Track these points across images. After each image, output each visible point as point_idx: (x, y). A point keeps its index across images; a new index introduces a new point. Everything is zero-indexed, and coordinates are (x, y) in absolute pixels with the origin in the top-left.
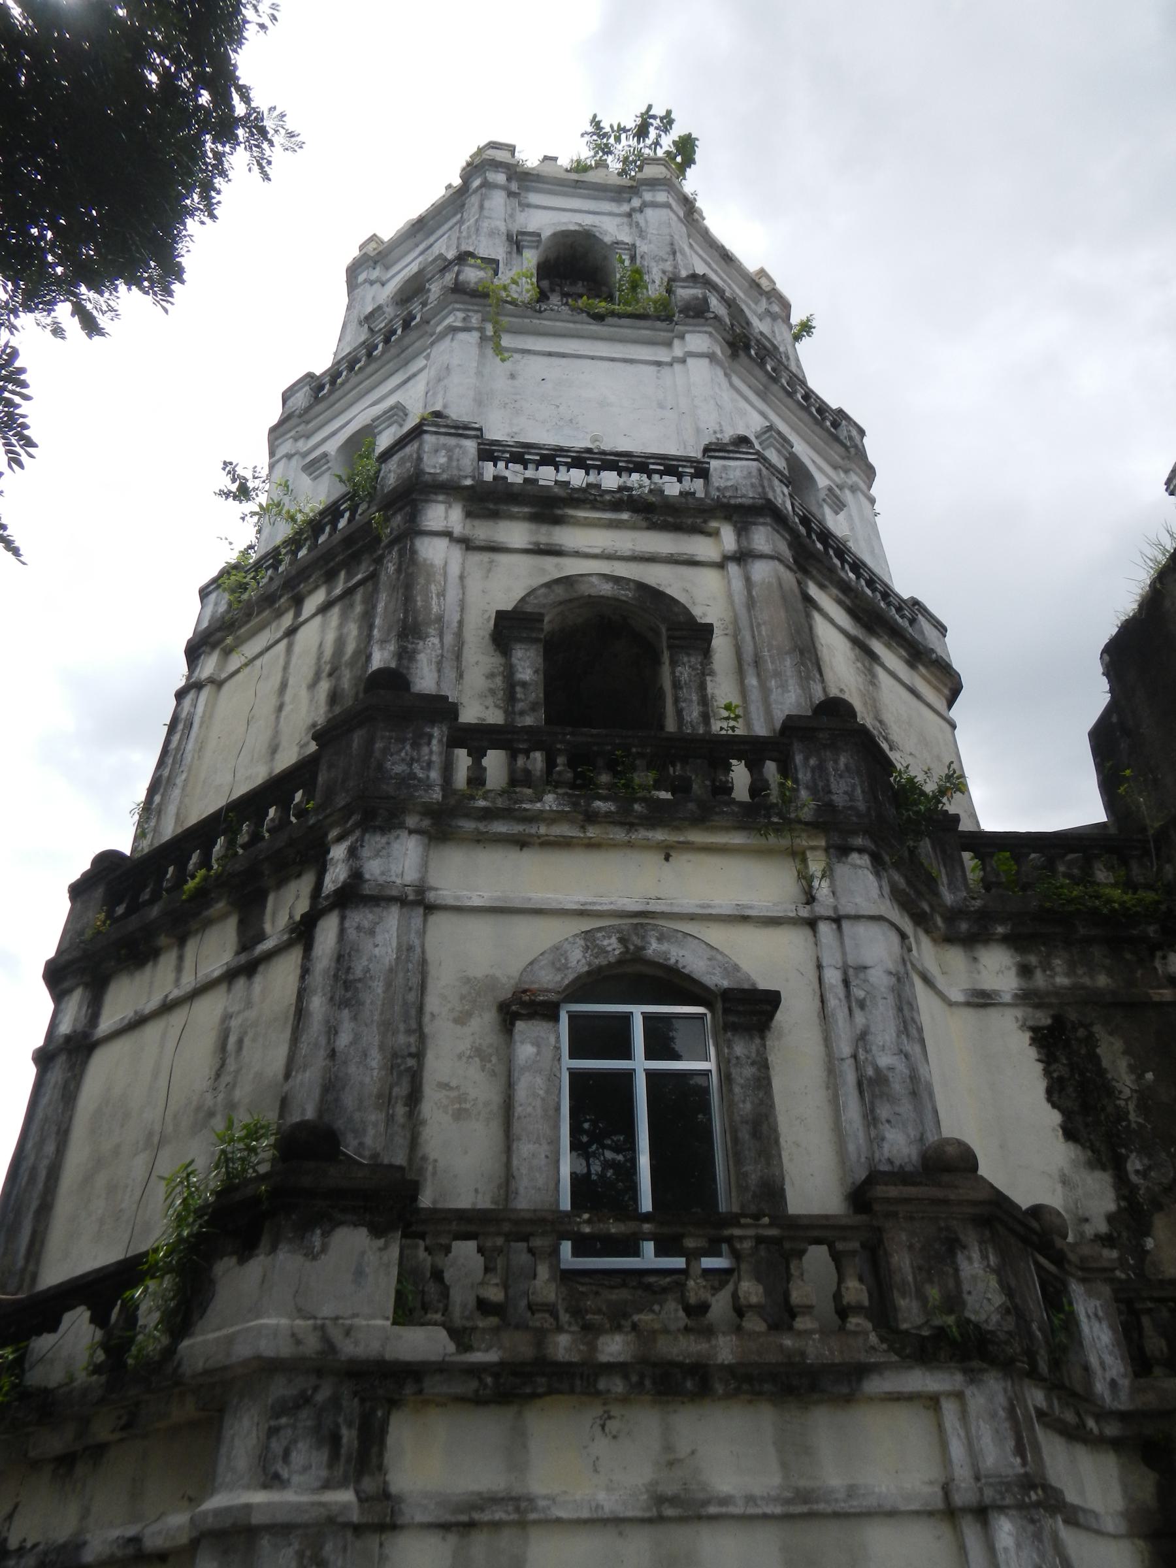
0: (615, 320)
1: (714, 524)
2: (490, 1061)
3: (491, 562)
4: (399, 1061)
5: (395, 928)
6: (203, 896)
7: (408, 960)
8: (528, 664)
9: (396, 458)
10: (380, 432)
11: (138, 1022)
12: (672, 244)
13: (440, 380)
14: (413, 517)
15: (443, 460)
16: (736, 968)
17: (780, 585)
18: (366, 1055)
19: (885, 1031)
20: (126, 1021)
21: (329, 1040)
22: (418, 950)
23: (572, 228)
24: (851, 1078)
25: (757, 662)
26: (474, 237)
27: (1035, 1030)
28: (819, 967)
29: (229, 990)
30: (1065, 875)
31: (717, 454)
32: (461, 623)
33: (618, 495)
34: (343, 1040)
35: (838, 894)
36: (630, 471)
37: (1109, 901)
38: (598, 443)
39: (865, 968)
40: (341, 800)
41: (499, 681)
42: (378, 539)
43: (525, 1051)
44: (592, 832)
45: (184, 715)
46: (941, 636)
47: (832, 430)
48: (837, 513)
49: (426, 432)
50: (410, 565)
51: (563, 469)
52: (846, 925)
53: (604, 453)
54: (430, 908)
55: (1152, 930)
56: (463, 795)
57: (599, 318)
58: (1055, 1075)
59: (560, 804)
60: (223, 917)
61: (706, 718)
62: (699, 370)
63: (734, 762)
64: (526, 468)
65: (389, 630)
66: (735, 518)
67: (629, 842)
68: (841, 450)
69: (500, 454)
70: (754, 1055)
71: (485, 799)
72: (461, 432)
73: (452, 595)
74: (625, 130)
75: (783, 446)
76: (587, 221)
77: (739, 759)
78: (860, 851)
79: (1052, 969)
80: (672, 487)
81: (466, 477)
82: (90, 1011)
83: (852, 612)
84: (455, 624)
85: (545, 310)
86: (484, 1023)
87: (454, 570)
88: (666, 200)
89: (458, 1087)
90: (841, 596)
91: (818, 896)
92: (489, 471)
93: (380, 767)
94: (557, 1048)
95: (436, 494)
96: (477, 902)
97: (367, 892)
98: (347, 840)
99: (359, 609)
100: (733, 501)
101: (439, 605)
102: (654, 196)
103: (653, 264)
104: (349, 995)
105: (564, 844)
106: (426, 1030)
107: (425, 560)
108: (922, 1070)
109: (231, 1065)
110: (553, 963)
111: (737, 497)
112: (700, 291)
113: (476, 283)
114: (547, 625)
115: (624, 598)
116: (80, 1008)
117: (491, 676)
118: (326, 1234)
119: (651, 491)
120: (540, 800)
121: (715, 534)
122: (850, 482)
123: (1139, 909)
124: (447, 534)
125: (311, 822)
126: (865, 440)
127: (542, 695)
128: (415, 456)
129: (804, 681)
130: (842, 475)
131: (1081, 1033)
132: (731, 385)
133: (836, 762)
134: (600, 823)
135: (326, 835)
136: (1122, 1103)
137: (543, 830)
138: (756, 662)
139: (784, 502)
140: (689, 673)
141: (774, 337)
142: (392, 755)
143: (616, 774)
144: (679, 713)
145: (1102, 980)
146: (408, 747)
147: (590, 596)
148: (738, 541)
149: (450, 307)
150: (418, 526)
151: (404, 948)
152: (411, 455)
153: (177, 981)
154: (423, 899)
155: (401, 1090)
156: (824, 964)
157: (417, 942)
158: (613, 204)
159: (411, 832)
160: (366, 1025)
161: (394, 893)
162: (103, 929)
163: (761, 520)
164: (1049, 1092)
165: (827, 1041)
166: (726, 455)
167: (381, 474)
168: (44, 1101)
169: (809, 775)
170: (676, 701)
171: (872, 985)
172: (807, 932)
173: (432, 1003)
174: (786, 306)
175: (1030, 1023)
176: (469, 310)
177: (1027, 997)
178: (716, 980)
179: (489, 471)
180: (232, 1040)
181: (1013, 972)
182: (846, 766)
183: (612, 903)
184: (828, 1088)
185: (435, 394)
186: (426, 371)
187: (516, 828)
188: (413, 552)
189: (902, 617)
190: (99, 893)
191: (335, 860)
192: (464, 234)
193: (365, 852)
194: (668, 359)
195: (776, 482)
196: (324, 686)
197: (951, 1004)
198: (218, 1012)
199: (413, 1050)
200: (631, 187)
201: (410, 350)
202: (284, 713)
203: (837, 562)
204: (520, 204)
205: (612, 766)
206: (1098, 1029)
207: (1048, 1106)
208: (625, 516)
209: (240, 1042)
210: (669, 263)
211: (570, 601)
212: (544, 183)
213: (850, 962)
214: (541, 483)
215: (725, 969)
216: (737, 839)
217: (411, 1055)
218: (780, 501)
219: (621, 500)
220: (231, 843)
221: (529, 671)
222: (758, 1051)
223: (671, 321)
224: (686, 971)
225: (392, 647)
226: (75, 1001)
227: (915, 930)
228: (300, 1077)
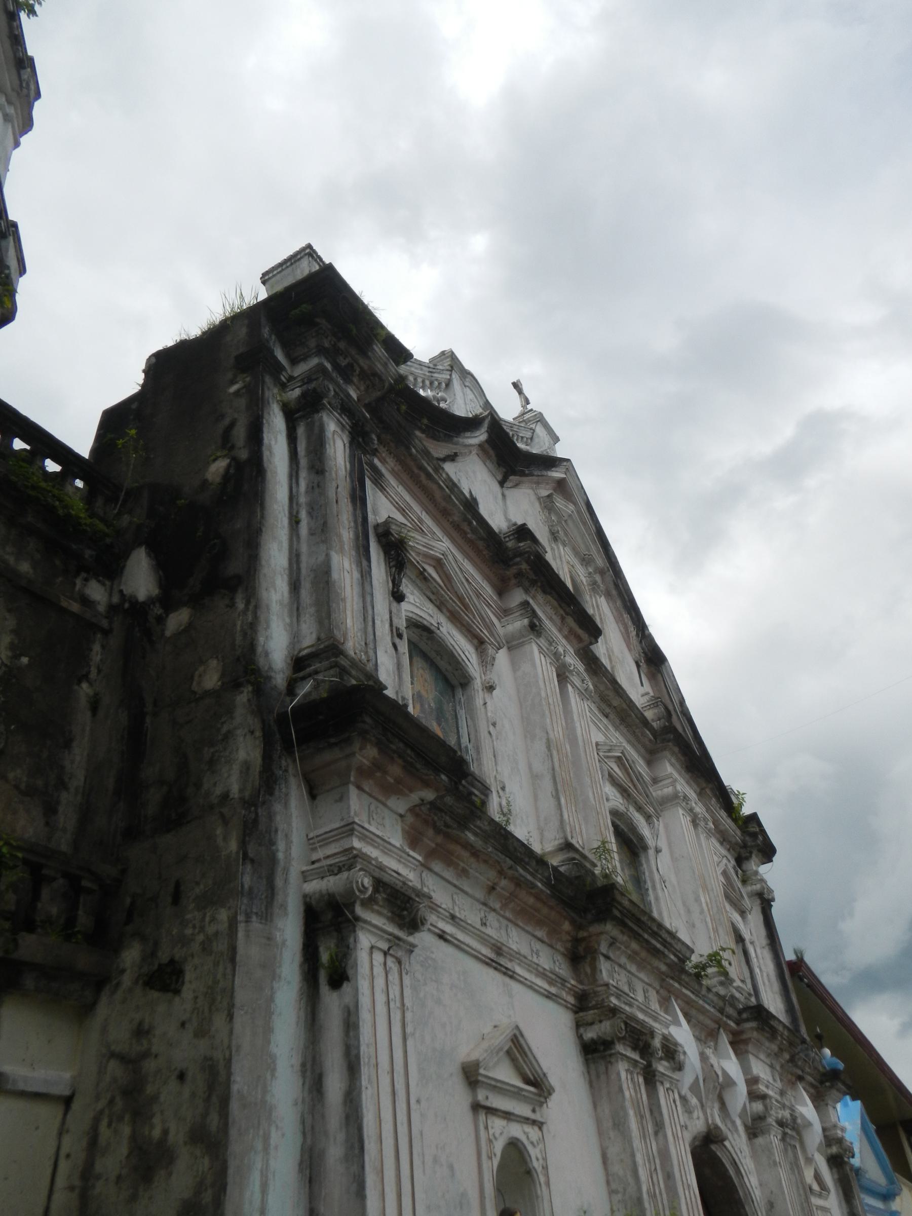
55: (88, 553)
68: (17, 82)
123: (88, 529)
145: (25, 567)
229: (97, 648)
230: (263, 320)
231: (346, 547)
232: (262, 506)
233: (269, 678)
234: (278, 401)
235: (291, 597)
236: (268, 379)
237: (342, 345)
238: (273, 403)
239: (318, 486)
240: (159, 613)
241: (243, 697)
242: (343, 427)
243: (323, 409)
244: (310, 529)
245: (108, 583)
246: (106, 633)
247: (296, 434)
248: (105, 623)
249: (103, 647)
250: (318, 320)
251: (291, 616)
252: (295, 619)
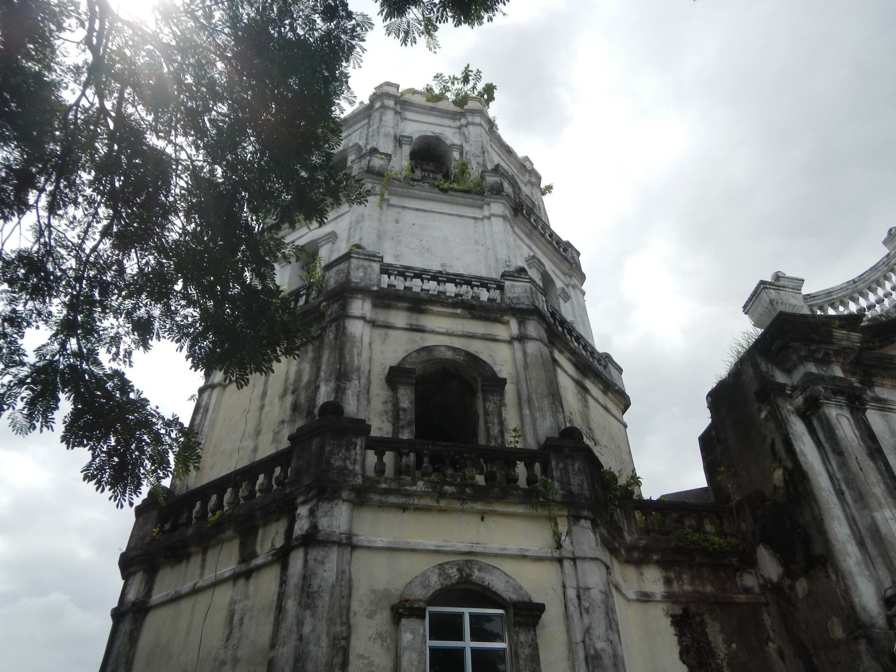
0: (454, 193)
1: (506, 318)
2: (386, 641)
3: (386, 334)
4: (337, 642)
5: (335, 560)
6: (219, 526)
7: (342, 580)
8: (406, 397)
9: (334, 270)
10: (321, 246)
11: (177, 598)
12: (483, 147)
13: (358, 222)
14: (344, 307)
15: (361, 274)
16: (521, 588)
17: (542, 356)
18: (319, 639)
19: (599, 628)
20: (169, 597)
21: (299, 628)
22: (347, 573)
23: (429, 134)
24: (581, 655)
25: (529, 401)
26: (376, 137)
27: (673, 616)
28: (564, 587)
29: (234, 585)
30: (689, 527)
31: (509, 278)
32: (369, 371)
33: (455, 300)
34: (307, 629)
35: (574, 544)
36: (461, 284)
37: (713, 543)
38: (444, 268)
39: (589, 589)
40: (306, 481)
41: (389, 406)
42: (323, 315)
43: (407, 637)
44: (443, 503)
45: (203, 404)
46: (619, 374)
47: (564, 254)
48: (566, 302)
49: (352, 257)
50: (342, 334)
51: (425, 281)
52: (578, 562)
53: (448, 274)
54: (354, 547)
56: (373, 481)
57: (445, 191)
58: (684, 644)
59: (426, 487)
60: (231, 539)
61: (502, 433)
62: (497, 223)
63: (518, 462)
64: (406, 280)
65: (331, 374)
66: (518, 316)
67: (462, 509)
68: (568, 265)
69: (392, 272)
70: (530, 641)
71: (386, 483)
72: (371, 258)
73: (365, 354)
74: (457, 79)
75: (540, 267)
76: (437, 130)
77: (521, 461)
78: (586, 518)
79: (682, 581)
80: (484, 295)
81: (374, 285)
82: (147, 587)
83: (576, 366)
84: (367, 372)
85: (416, 185)
86: (383, 618)
87: (366, 340)
88: (479, 121)
89: (368, 658)
90: (571, 357)
91: (563, 545)
92: (385, 280)
93: (328, 462)
94: (424, 636)
95: (357, 294)
96: (380, 544)
97: (321, 538)
98: (308, 504)
99: (310, 355)
100: (517, 306)
101: (359, 361)
102: (473, 119)
103: (472, 158)
104: (310, 601)
105: (427, 509)
106: (352, 622)
107: (351, 333)
108: (619, 650)
109: (236, 634)
110: (422, 583)
111: (518, 304)
112: (498, 179)
113: (379, 168)
114: (417, 374)
115: (458, 361)
116: (141, 584)
117: (385, 403)
119: (473, 297)
120: (415, 485)
121: (507, 323)
122: (572, 283)
123: (728, 548)
124: (363, 318)
125: (288, 491)
126: (580, 258)
127: (414, 417)
128: (346, 271)
129: (554, 413)
130: (569, 279)
131: (698, 619)
132: (514, 232)
133: (573, 465)
134: (447, 498)
135: (295, 499)
136: (719, 661)
137: (416, 501)
138: (528, 401)
139: (543, 306)
140: (493, 407)
141: (533, 196)
142: (334, 455)
143: (456, 470)
144: (488, 430)
145: (709, 589)
146: (343, 451)
147: (440, 358)
148: (519, 329)
150: (347, 312)
151: (340, 572)
152: (344, 270)
153: (202, 575)
154: (351, 542)
155: (338, 660)
156: (567, 586)
157: (347, 568)
158: (451, 121)
159: (344, 501)
160: (319, 620)
161: (335, 539)
162: (157, 538)
163: (532, 317)
164: (681, 654)
165: (569, 631)
166: (513, 278)
167: (326, 278)
168: (118, 642)
169: (559, 473)
170: (486, 422)
171: (592, 599)
172: (557, 565)
173: (355, 606)
174: (539, 178)
175: (670, 612)
176: (375, 183)
177: (669, 597)
178: (510, 595)
179: (385, 280)
180: (237, 617)
181: (661, 582)
182: (579, 468)
183: (453, 546)
184: (569, 660)
185: (355, 230)
186: (349, 215)
187: (402, 500)
188: (344, 328)
189: (600, 365)
190: (154, 513)
191: (300, 516)
192: (371, 134)
193: (319, 513)
194: (481, 216)
195: (539, 294)
196: (289, 399)
197: (628, 600)
198: (227, 599)
199: (345, 635)
200: (461, 113)
202: (264, 411)
203: (568, 337)
204: (401, 118)
205: (453, 464)
206: (707, 618)
207: (681, 662)
208: (459, 311)
209: (242, 619)
210: (481, 158)
211: (429, 361)
212: (413, 106)
213: (581, 585)
214: (414, 290)
216: (520, 509)
217: (344, 638)
218: (541, 305)
219: (457, 302)
220: (236, 493)
221: (407, 402)
222: (532, 638)
223: (483, 195)
224: (493, 589)
225: (332, 385)
226: (138, 580)
227: (611, 558)
228: (281, 650)
229: (766, 617)
230: (759, 359)
231: (883, 501)
232: (816, 501)
233: (873, 625)
234: (793, 412)
235: (862, 554)
236: (780, 401)
237: (813, 347)
238: (790, 416)
239: (844, 465)
240: (789, 584)
241: (862, 646)
242: (841, 407)
243: (822, 405)
244: (853, 498)
245: (753, 571)
246: (767, 605)
247: (814, 426)
248: (763, 599)
249: (769, 614)
250: (791, 345)
251: (868, 568)
252: (872, 568)
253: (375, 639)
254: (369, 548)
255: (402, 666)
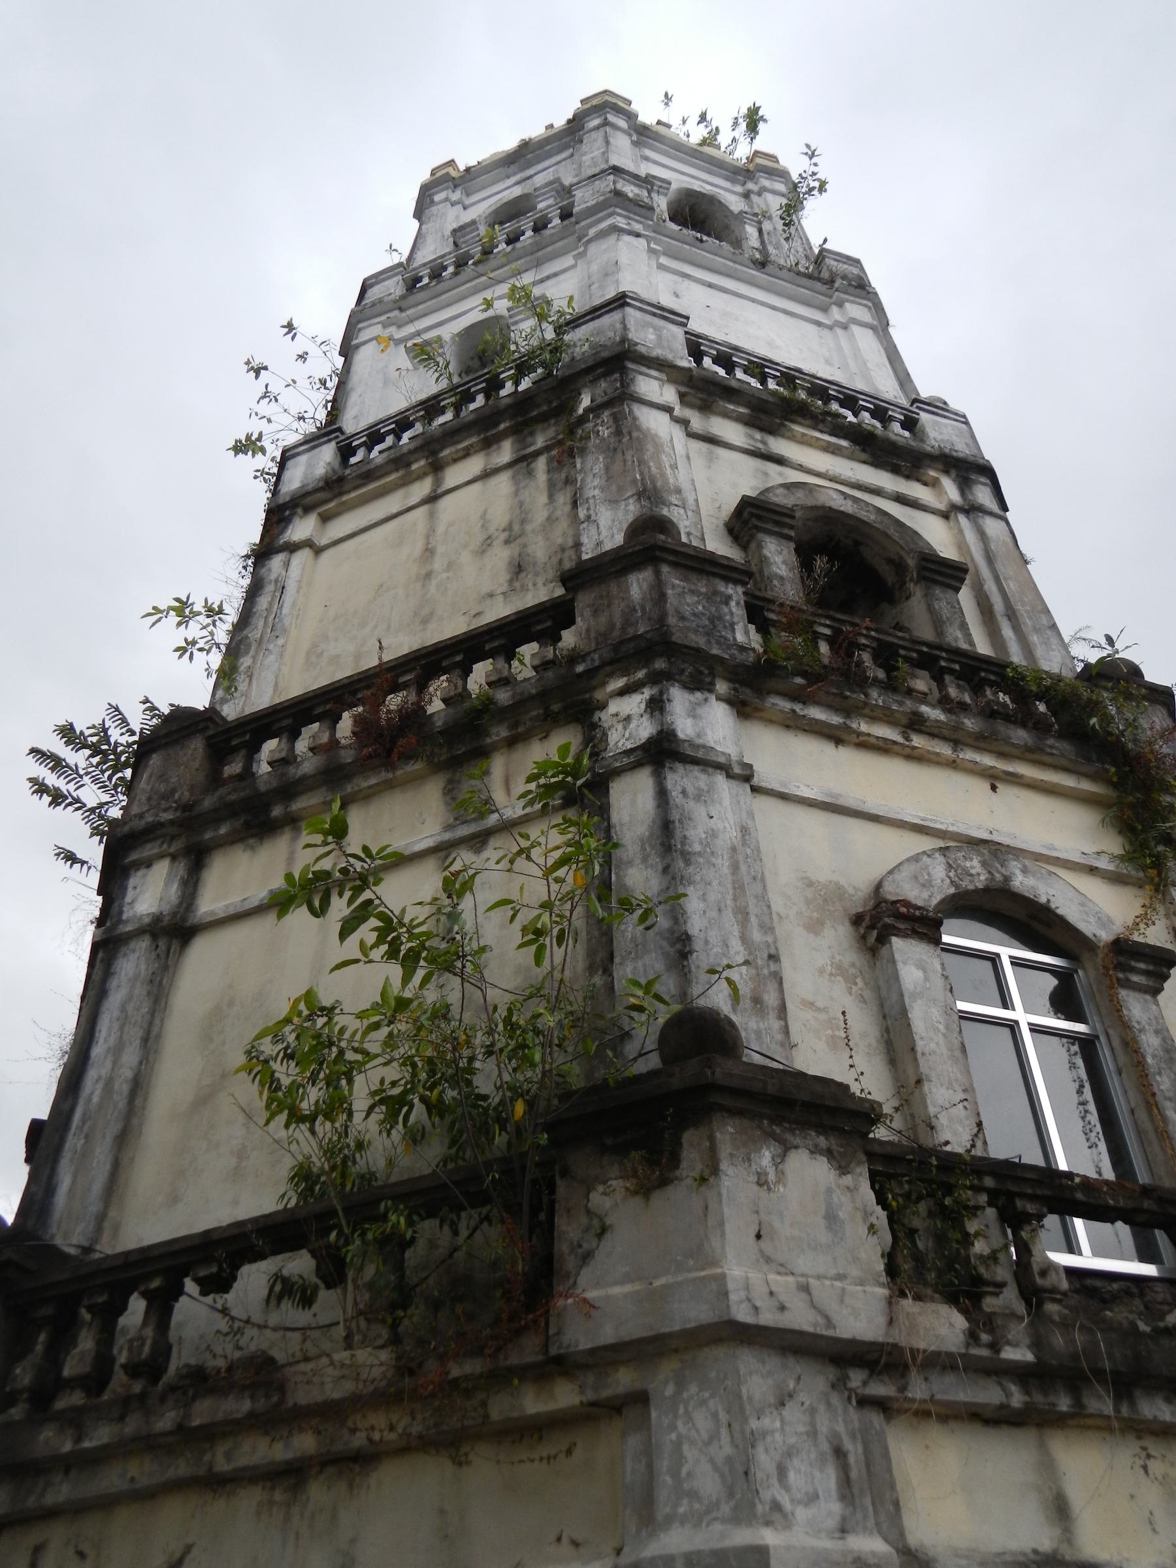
2: (856, 984)
25: (1012, 615)
44: (918, 741)
49: (629, 305)
67: (954, 761)
76: (707, 189)
105: (883, 748)
107: (648, 429)
118: (779, 1160)
147: (830, 508)
149: (611, 210)
201: (549, 249)
208: (844, 443)
215: (1099, 918)
253: (831, 974)
254: (784, 797)
255: (914, 1030)
